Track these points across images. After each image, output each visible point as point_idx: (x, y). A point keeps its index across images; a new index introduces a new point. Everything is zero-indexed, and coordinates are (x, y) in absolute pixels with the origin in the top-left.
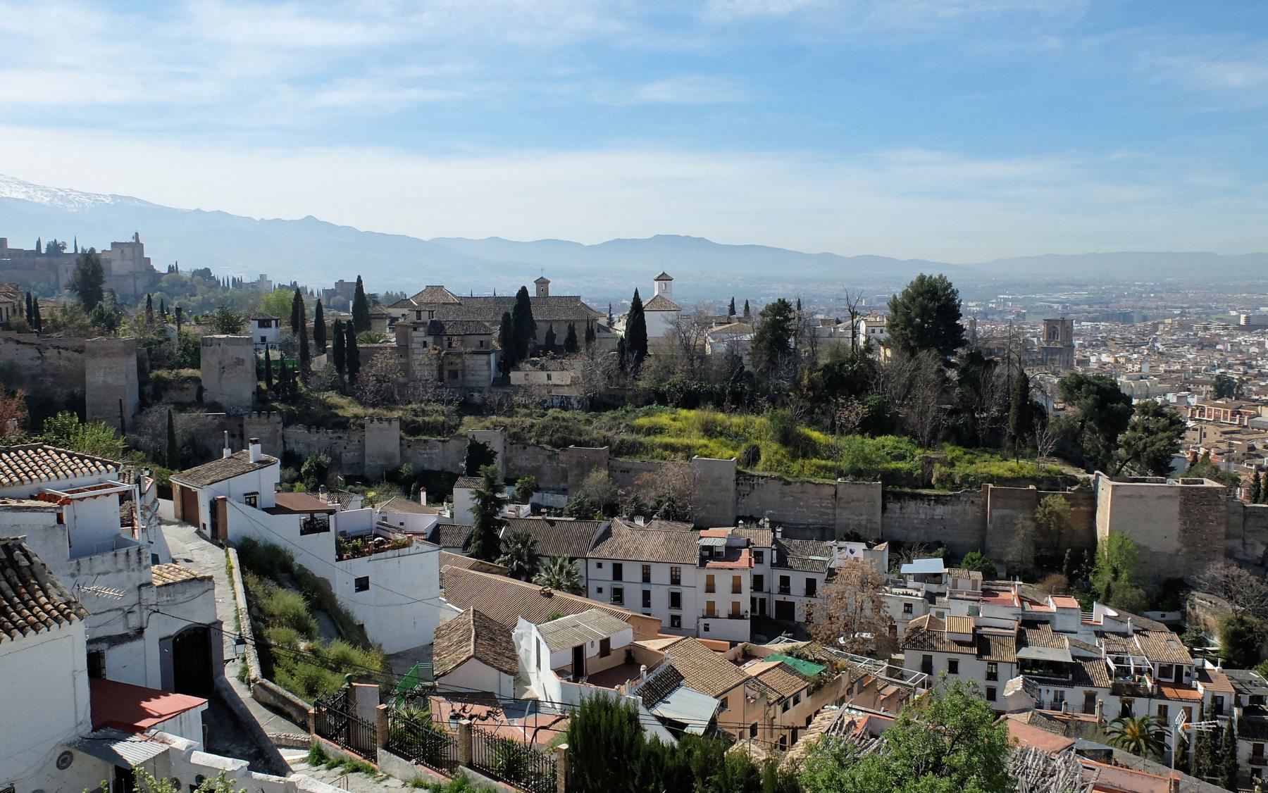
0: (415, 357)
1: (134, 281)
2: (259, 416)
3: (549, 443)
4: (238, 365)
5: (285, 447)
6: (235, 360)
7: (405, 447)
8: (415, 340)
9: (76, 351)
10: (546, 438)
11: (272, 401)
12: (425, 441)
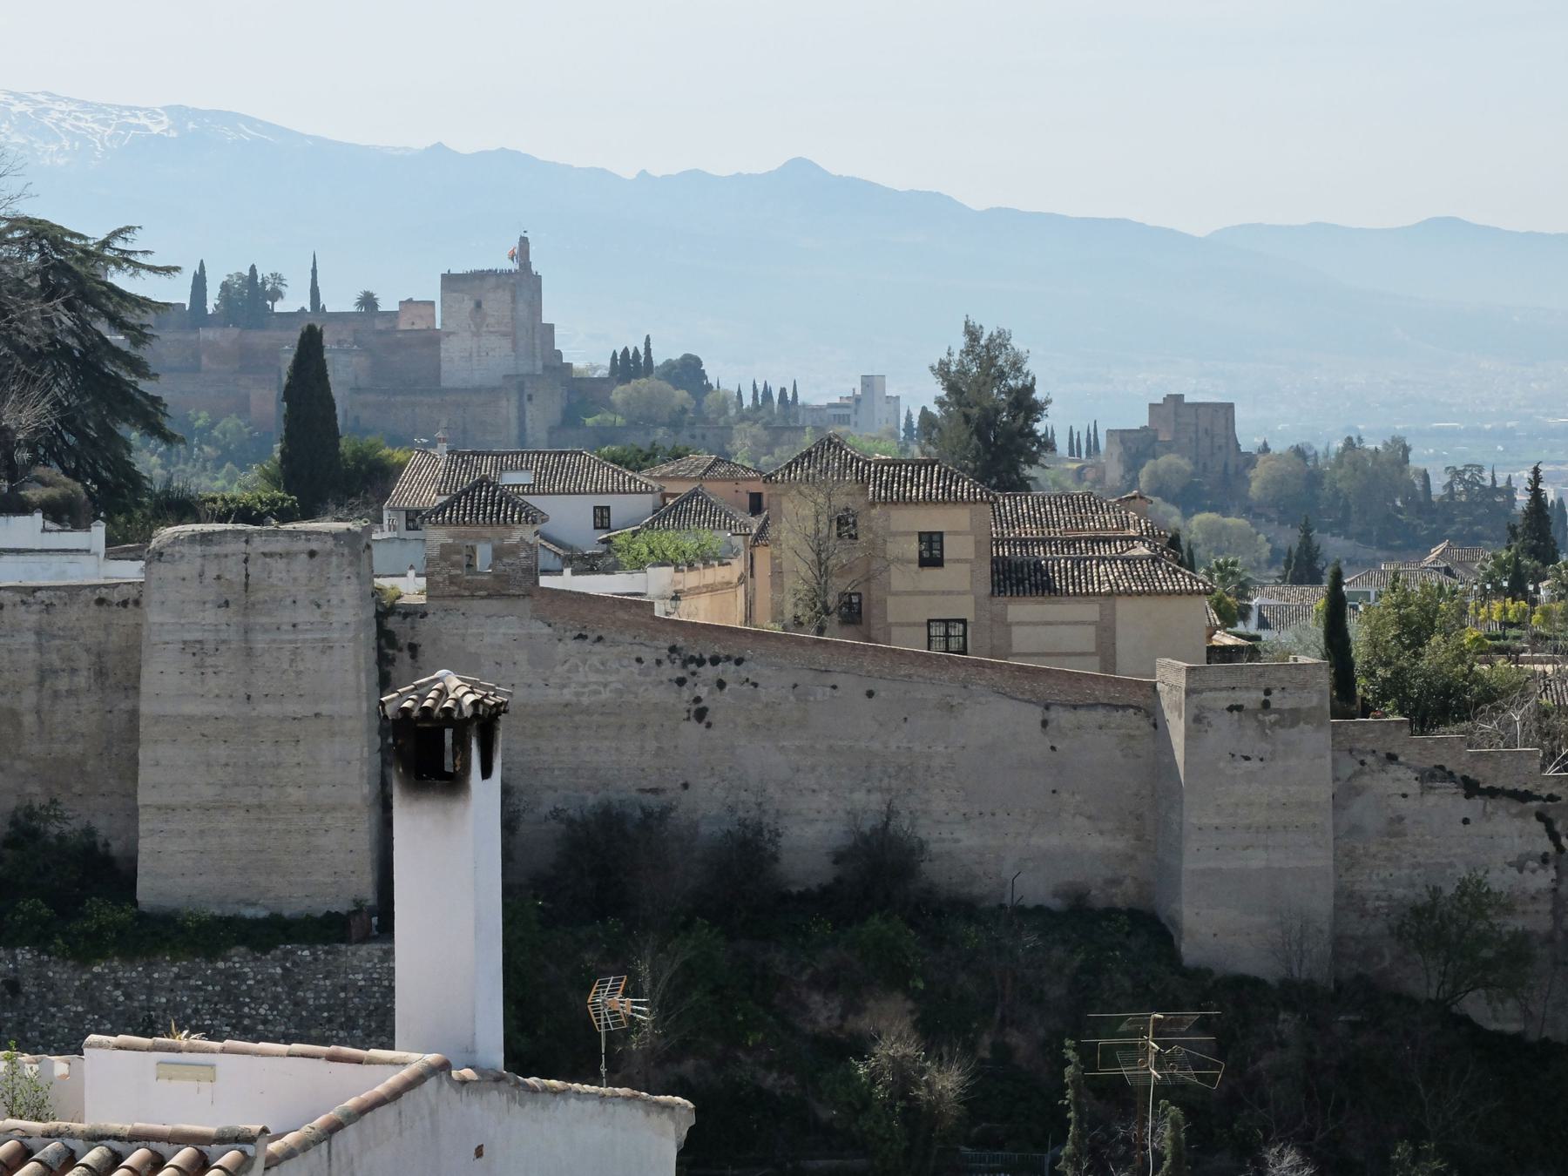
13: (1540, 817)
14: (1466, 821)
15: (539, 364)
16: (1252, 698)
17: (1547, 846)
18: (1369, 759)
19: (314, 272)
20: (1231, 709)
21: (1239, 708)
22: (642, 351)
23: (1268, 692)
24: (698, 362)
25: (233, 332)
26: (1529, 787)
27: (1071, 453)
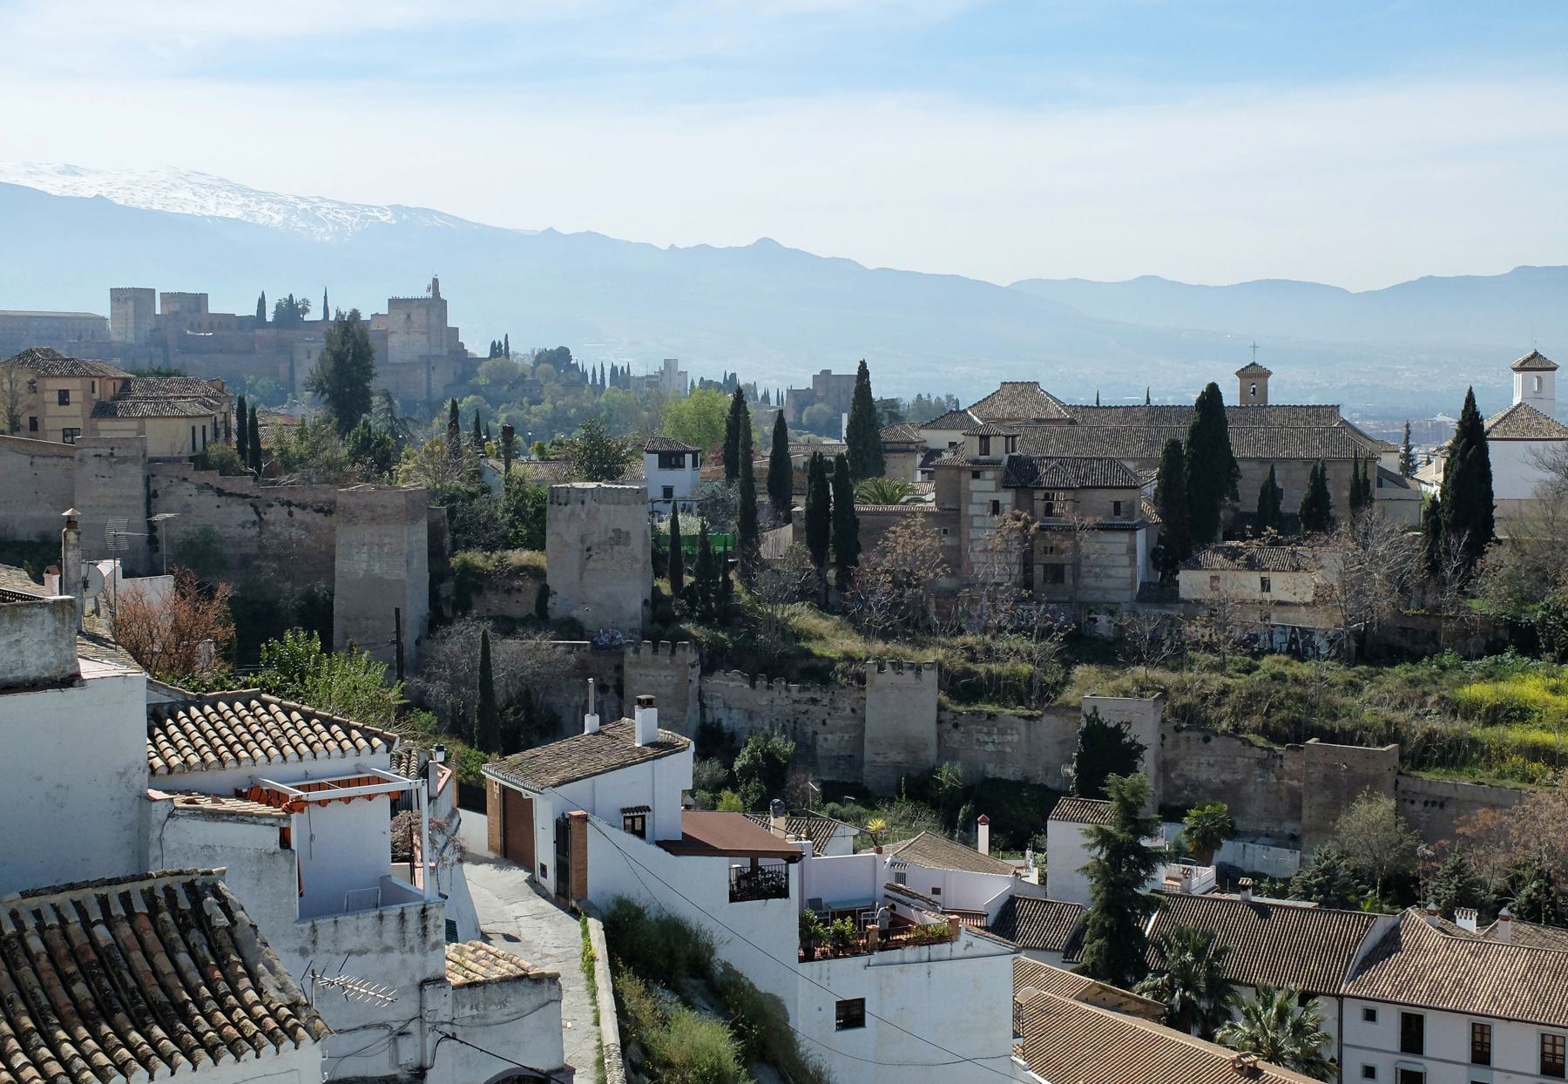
0: (973, 535)
1: (429, 374)
2: (655, 651)
3: (1264, 731)
4: (618, 544)
5: (703, 715)
6: (611, 534)
7: (949, 726)
8: (976, 497)
9: (320, 510)
10: (1256, 720)
11: (679, 620)
12: (991, 716)
13: (252, 505)
14: (218, 507)
15: (445, 349)
16: (105, 451)
17: (255, 517)
18: (174, 480)
19: (326, 298)
20: (96, 456)
21: (100, 456)
22: (503, 343)
23: (112, 449)
24: (568, 351)
25: (273, 332)
26: (248, 492)
27: (778, 404)
